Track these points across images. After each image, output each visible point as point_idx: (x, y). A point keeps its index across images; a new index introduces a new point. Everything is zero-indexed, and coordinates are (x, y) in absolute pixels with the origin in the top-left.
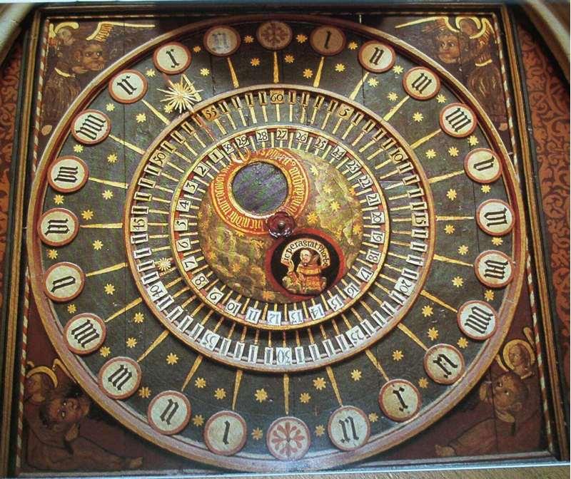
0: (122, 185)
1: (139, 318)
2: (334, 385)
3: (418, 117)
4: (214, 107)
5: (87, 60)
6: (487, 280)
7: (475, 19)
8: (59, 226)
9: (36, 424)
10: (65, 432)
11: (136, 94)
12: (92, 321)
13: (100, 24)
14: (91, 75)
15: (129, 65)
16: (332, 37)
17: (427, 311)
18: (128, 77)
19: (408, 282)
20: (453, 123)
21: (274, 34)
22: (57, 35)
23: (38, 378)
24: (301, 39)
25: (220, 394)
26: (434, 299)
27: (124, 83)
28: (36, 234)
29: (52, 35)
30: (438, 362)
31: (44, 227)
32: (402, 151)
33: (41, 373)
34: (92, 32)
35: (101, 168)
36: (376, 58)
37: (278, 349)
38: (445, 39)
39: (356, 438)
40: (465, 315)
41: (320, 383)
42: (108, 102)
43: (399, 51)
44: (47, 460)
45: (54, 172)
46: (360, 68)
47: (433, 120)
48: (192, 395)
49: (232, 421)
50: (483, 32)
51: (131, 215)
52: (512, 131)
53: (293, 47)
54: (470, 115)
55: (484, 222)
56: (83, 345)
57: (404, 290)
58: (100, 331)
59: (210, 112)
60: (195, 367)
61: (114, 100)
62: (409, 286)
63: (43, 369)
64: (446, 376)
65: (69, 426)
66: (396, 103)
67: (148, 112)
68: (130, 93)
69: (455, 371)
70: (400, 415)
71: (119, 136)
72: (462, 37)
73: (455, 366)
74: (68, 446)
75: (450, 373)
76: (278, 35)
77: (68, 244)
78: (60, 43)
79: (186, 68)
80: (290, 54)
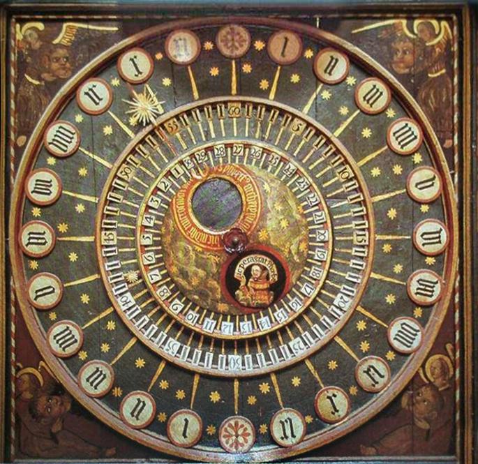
0: (92, 199)
1: (111, 325)
2: (277, 390)
3: (367, 133)
4: (175, 120)
5: (55, 66)
6: (417, 298)
7: (434, 22)
8: (37, 238)
9: (26, 418)
10: (51, 425)
11: (103, 105)
12: (71, 328)
13: (65, 25)
14: (59, 82)
15: (95, 73)
16: (289, 43)
17: (361, 326)
18: (94, 86)
19: (346, 298)
20: (400, 139)
21: (233, 40)
22: (25, 37)
23: (26, 378)
24: (259, 45)
25: (180, 395)
26: (368, 314)
27: (91, 93)
28: (18, 245)
29: (19, 37)
30: (367, 372)
31: (24, 239)
32: (349, 169)
33: (29, 374)
34: (57, 35)
35: (70, 181)
36: (330, 69)
37: (230, 356)
38: (400, 46)
39: (293, 436)
40: (394, 330)
41: (265, 388)
42: (76, 113)
43: (354, 61)
44: (37, 449)
45: (31, 185)
46: (315, 79)
47: (381, 136)
48: (156, 394)
49: (191, 418)
50: (441, 37)
51: (102, 229)
52: (456, 148)
53: (251, 54)
54: (416, 130)
55: (419, 241)
56: (64, 349)
57: (342, 305)
58: (77, 337)
59: (172, 125)
60: (160, 370)
61: (82, 110)
62: (346, 302)
63: (30, 370)
64: (374, 386)
65: (54, 420)
66: (347, 117)
67: (115, 125)
68: (97, 104)
69: (381, 381)
70: (332, 417)
71: (88, 149)
72: (419, 43)
73: (382, 376)
74: (54, 437)
75: (377, 383)
76: (237, 41)
77: (46, 256)
78: (28, 46)
79: (149, 77)
80: (247, 63)
